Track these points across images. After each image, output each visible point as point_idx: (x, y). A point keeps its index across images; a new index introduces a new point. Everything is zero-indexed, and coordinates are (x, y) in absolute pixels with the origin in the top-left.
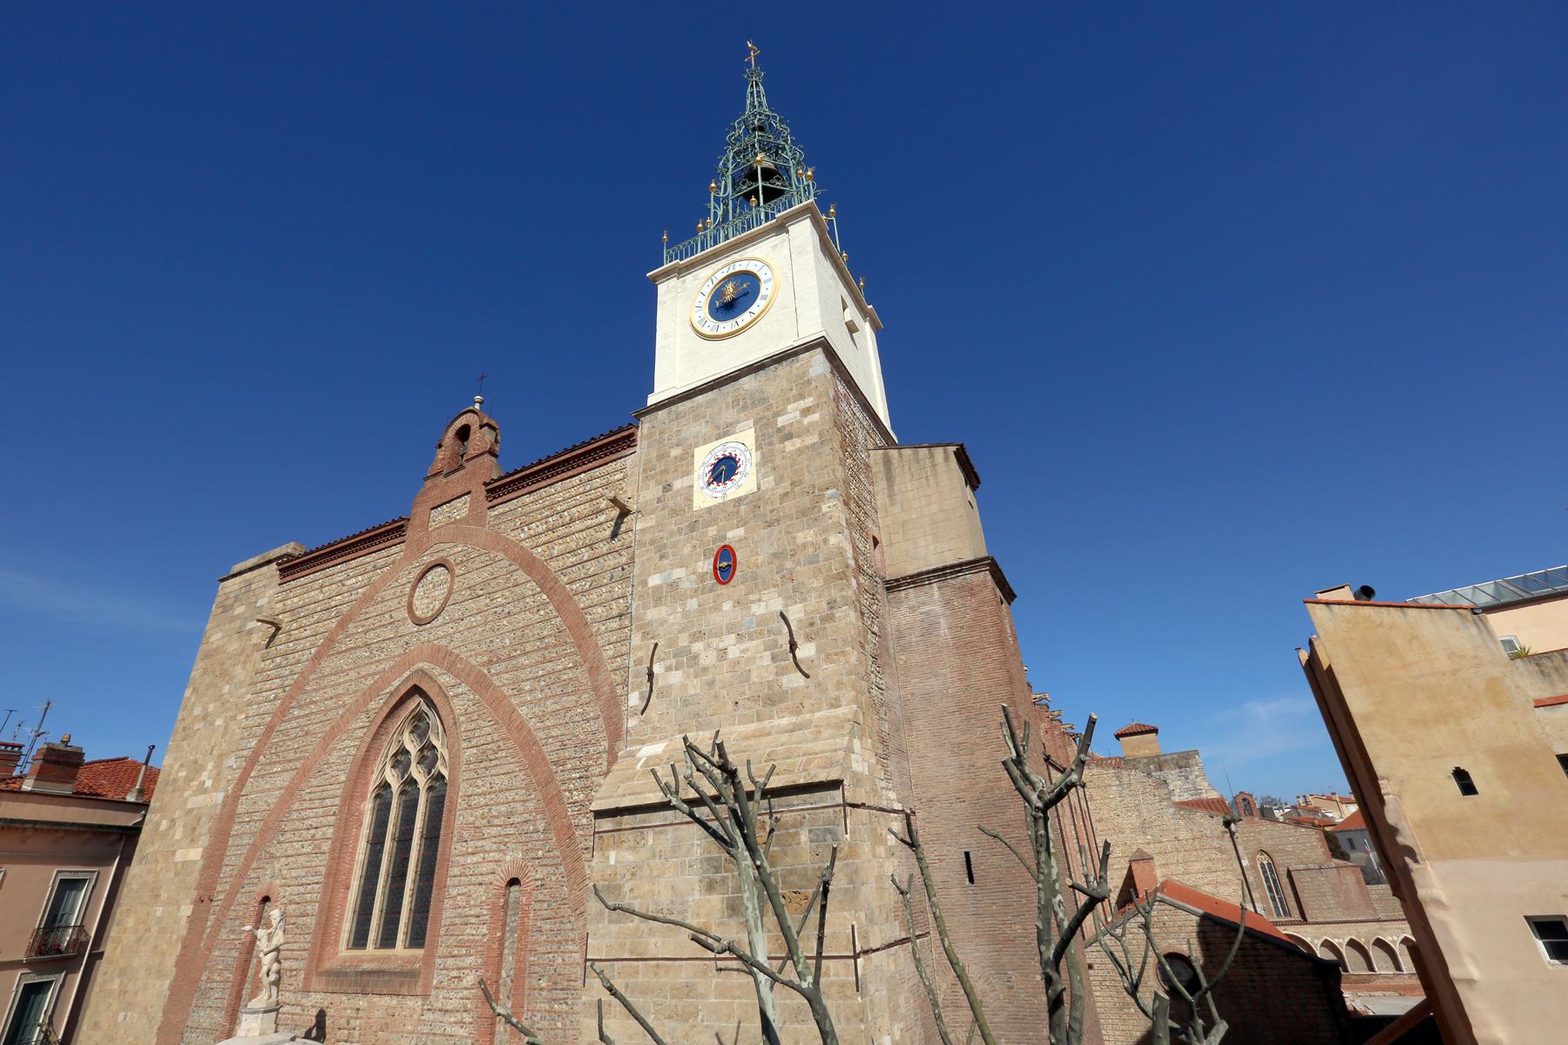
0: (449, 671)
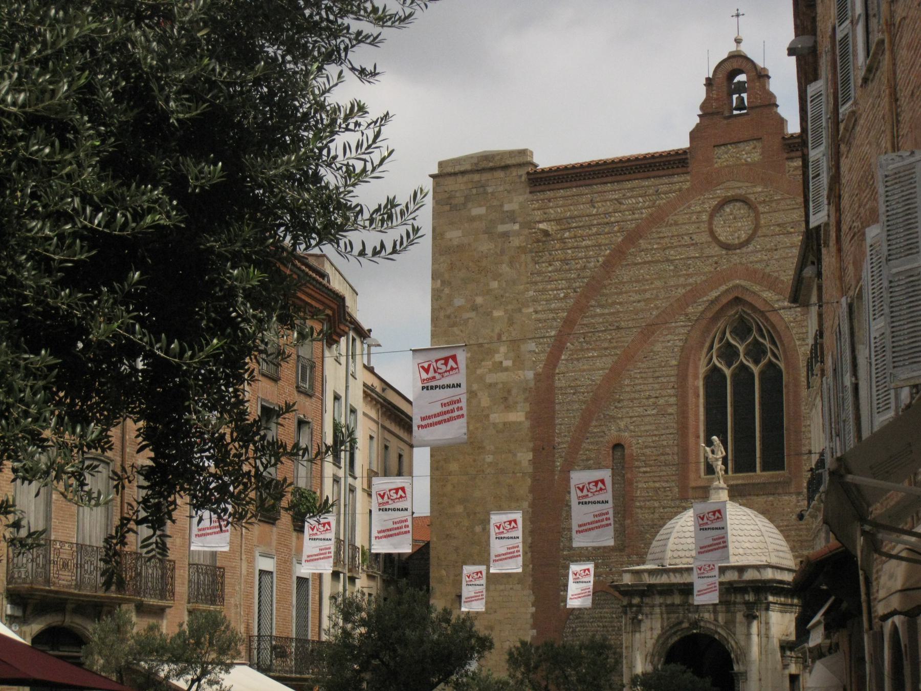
0: (770, 288)
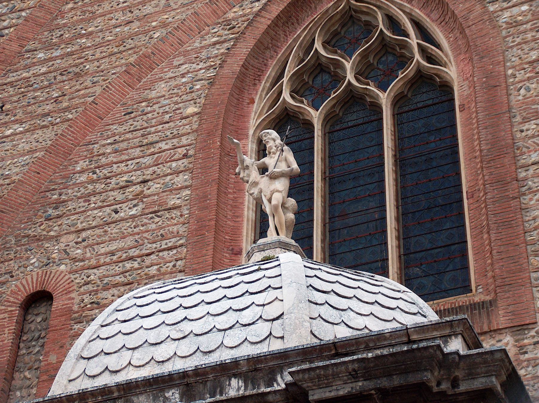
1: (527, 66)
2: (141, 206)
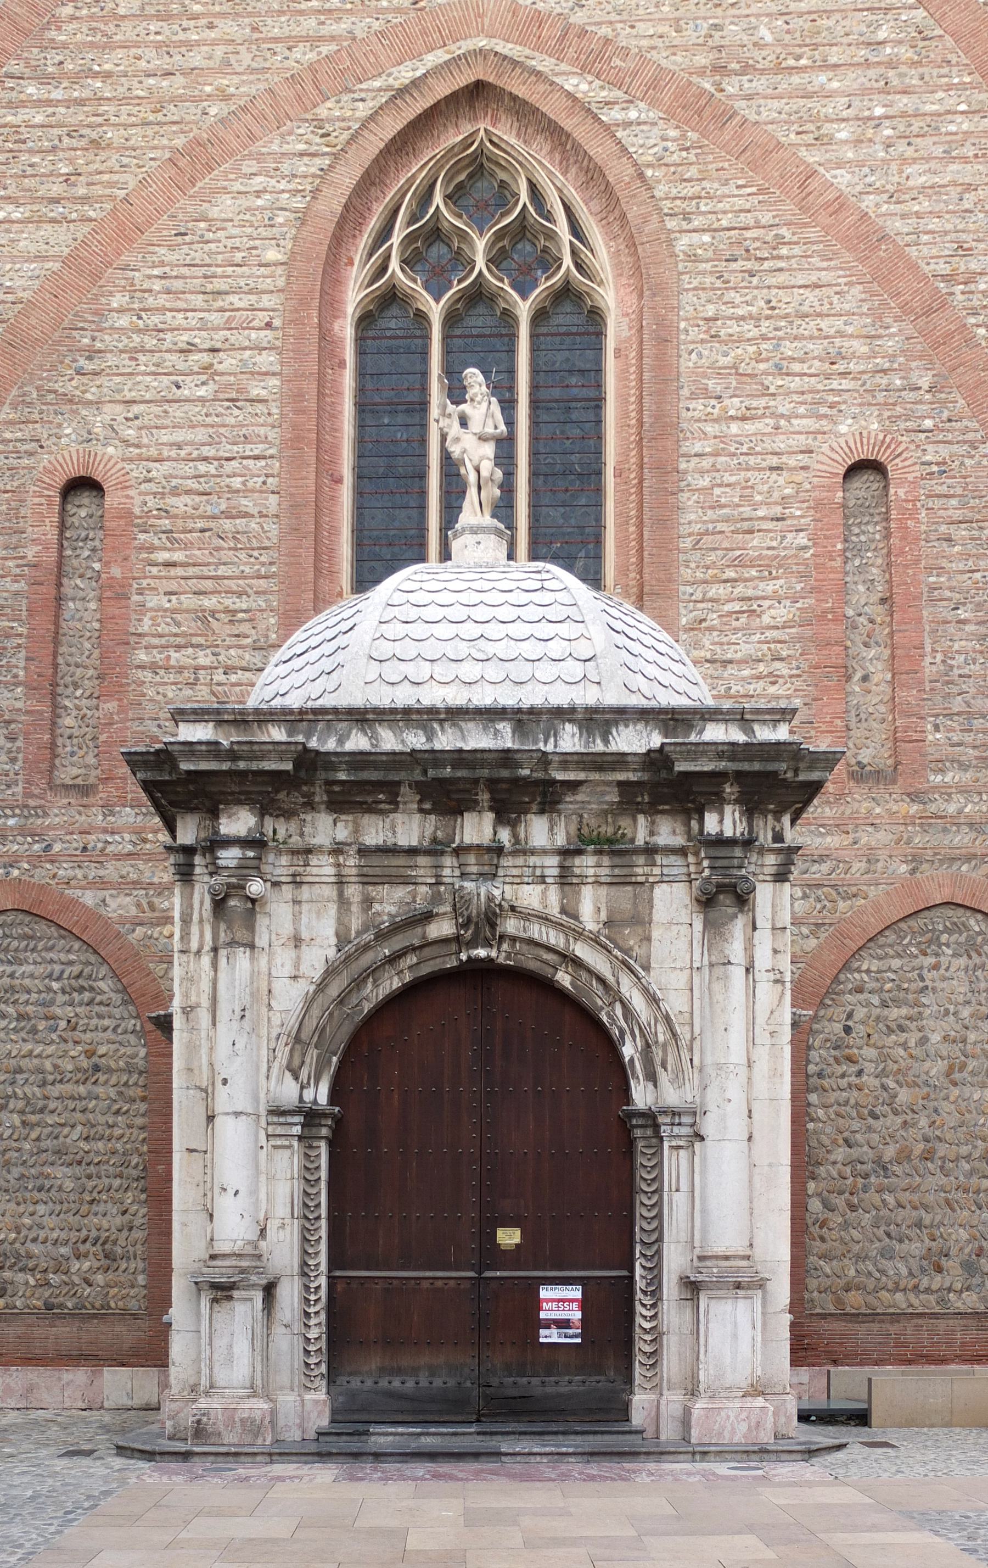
0: (584, 69)
1: (701, 323)
2: (211, 387)
